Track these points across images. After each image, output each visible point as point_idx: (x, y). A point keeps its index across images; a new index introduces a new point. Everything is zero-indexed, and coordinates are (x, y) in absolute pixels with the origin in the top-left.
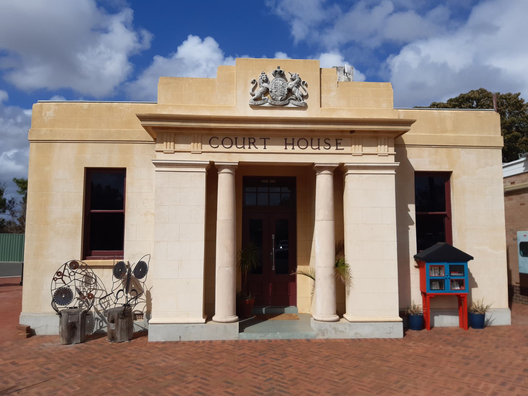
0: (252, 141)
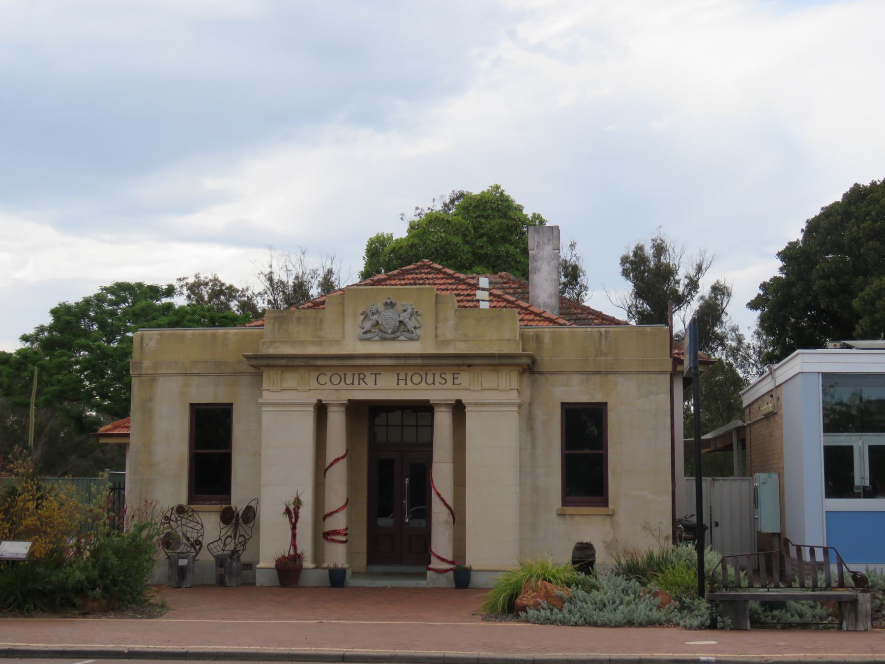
0: (362, 376)
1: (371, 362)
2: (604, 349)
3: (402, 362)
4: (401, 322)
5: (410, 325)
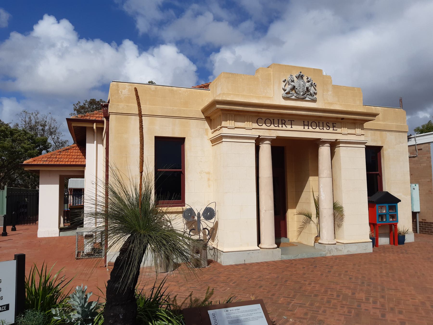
0: (283, 122)
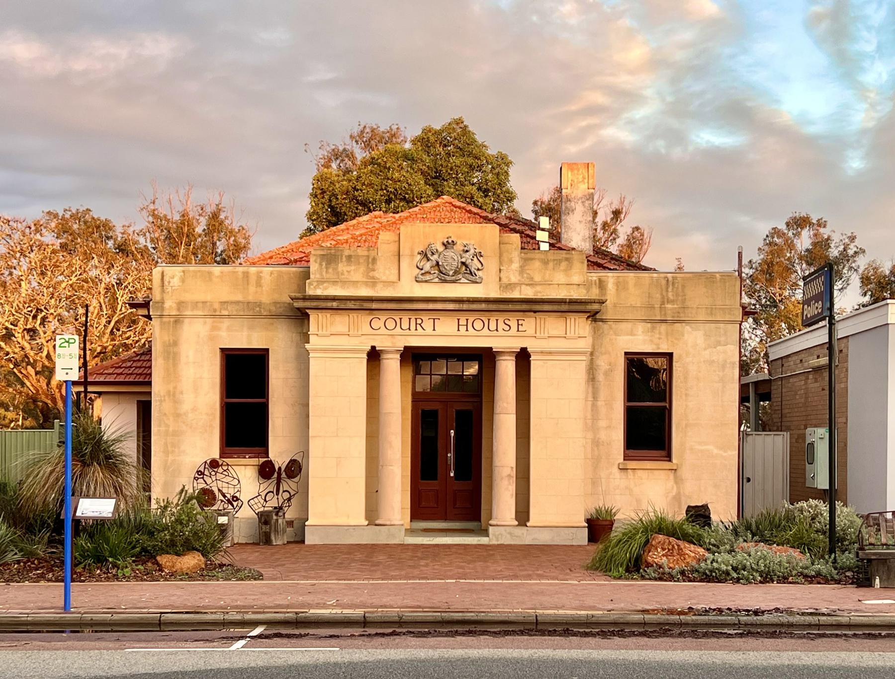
0: (419, 321)
1: (431, 306)
2: (671, 297)
3: (465, 306)
4: (463, 263)
5: (475, 264)
